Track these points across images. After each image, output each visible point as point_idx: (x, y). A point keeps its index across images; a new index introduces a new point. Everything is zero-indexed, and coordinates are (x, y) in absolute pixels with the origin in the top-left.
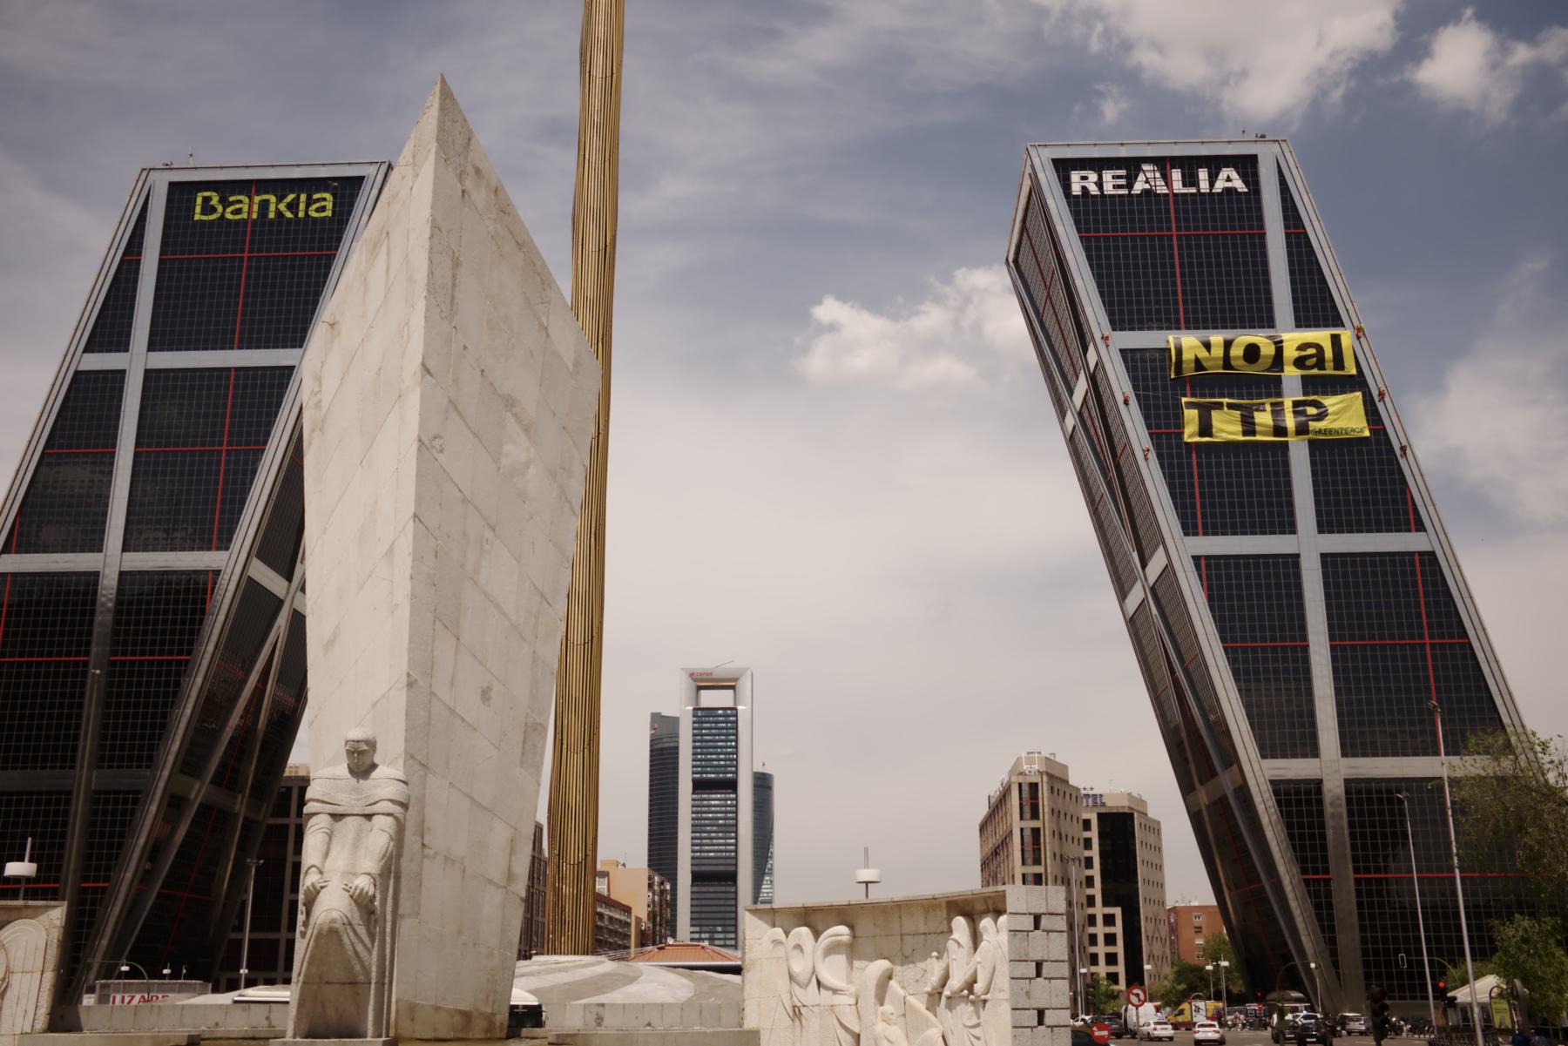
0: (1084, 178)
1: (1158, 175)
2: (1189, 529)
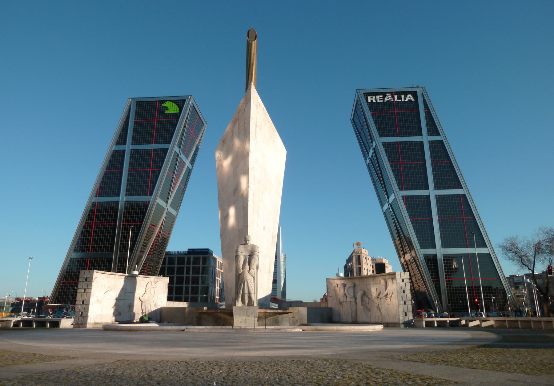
2: (401, 188)
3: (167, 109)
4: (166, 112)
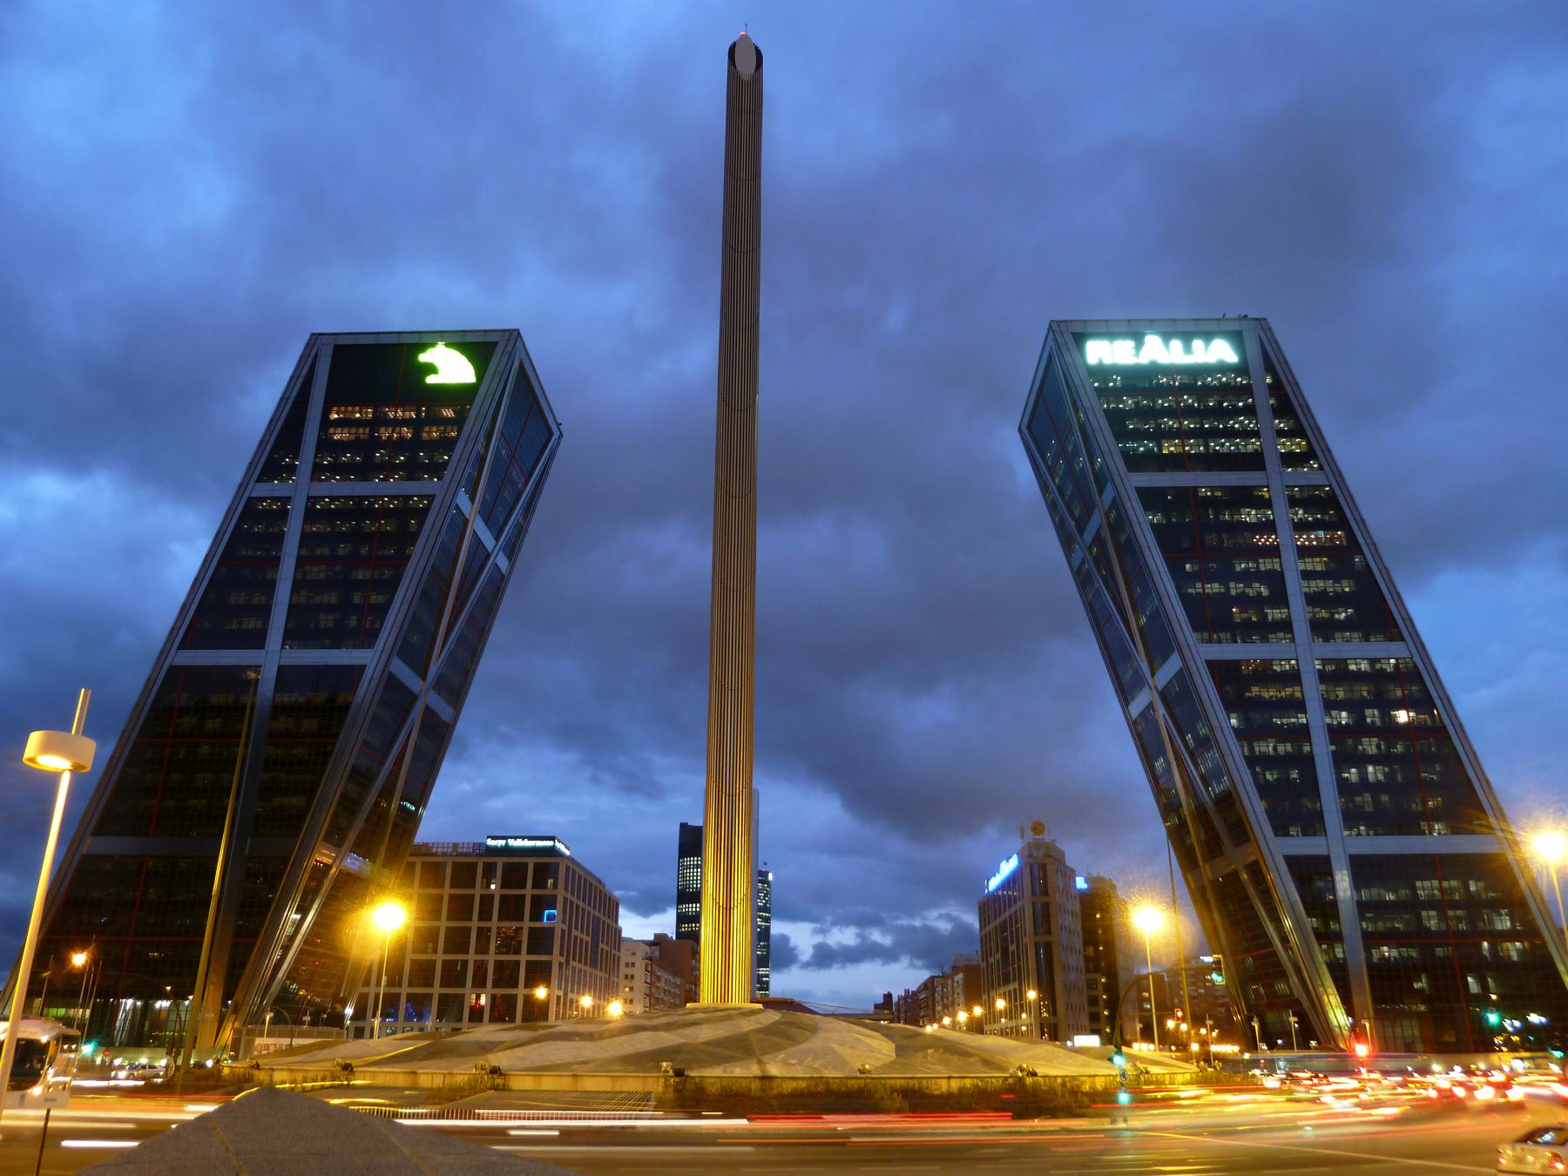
3: (431, 369)
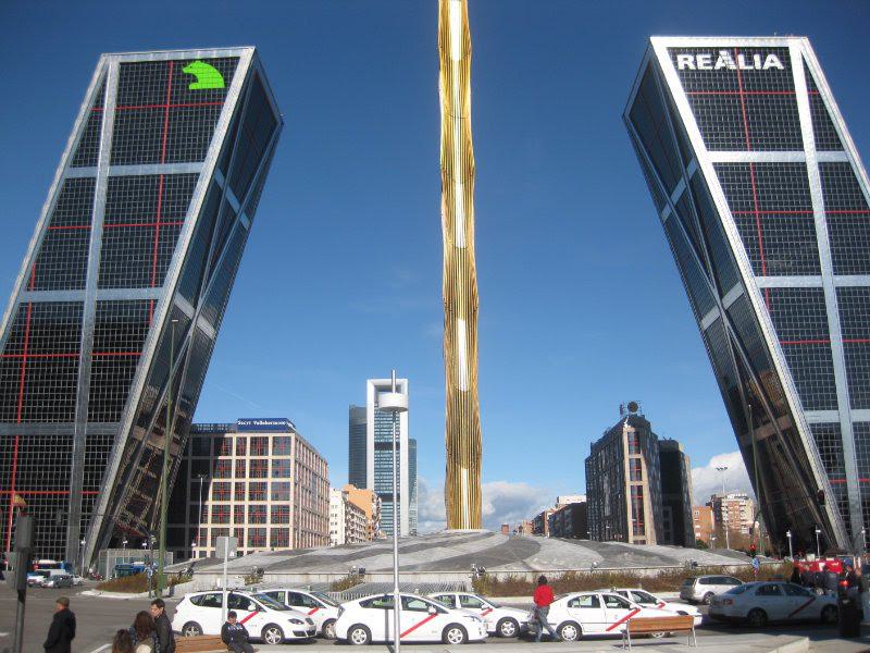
0: (686, 59)
1: (730, 58)
3: (195, 80)
4: (193, 86)
